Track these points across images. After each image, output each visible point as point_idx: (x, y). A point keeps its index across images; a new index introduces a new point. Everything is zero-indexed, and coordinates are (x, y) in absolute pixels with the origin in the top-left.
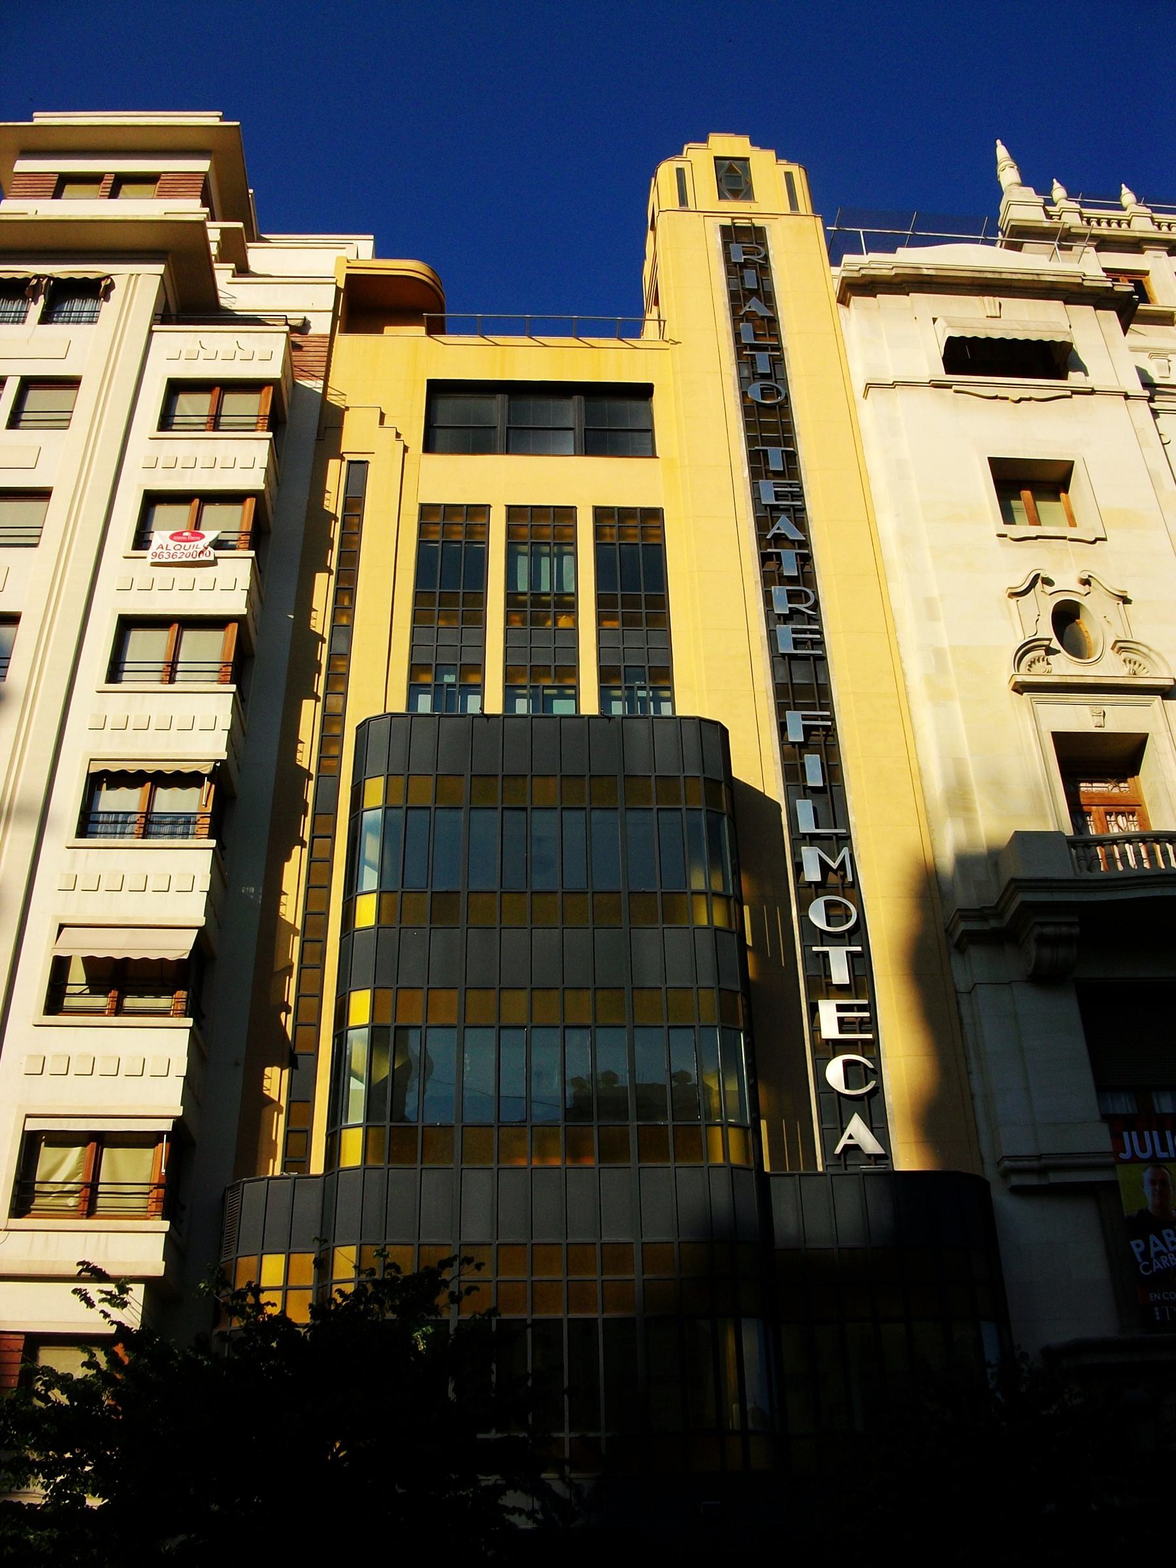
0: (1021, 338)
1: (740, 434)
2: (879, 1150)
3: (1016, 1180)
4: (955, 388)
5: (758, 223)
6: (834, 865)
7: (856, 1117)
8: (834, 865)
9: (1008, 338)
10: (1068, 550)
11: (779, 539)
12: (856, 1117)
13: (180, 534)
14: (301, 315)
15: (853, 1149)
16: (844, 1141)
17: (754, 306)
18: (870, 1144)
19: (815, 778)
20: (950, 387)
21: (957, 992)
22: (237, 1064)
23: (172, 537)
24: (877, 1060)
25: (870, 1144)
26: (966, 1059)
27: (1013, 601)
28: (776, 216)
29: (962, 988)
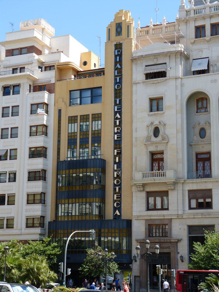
2: (119, 214)
5: (121, 42)
11: (117, 118)
15: (116, 214)
16: (115, 213)
18: (118, 214)
19: (117, 161)
24: (121, 203)
25: (118, 214)
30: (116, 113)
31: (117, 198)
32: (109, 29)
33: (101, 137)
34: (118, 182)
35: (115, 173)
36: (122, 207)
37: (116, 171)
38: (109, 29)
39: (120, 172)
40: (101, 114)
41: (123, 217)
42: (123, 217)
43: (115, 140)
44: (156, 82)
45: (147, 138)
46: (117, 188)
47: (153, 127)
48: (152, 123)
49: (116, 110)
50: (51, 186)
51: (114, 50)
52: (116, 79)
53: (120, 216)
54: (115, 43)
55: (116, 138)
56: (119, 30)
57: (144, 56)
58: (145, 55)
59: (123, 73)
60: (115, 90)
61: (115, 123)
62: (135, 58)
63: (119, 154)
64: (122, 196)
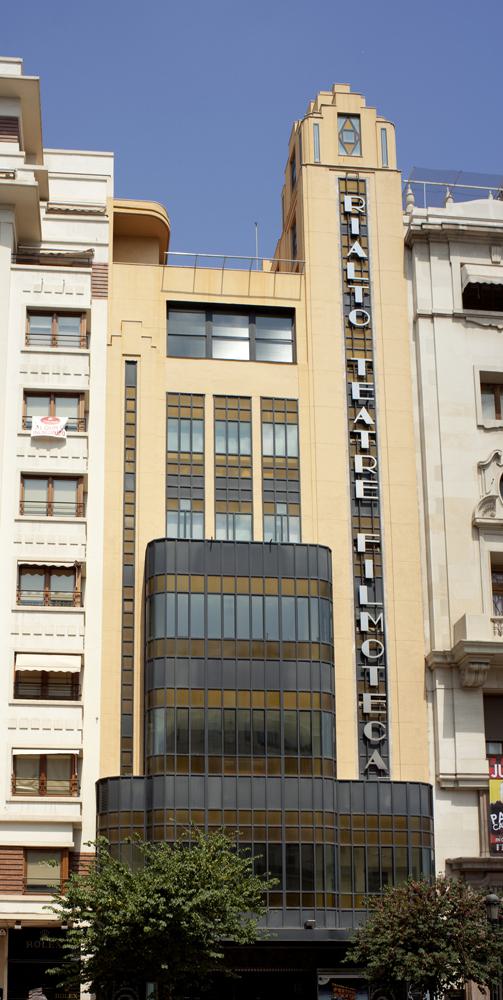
6: (376, 623)
8: (376, 623)
11: (362, 424)
13: (46, 419)
16: (370, 762)
17: (357, 248)
23: (42, 420)
30: (354, 405)
34: (375, 648)
54: (343, 175)
55: (360, 494)
59: (374, 277)
63: (374, 547)
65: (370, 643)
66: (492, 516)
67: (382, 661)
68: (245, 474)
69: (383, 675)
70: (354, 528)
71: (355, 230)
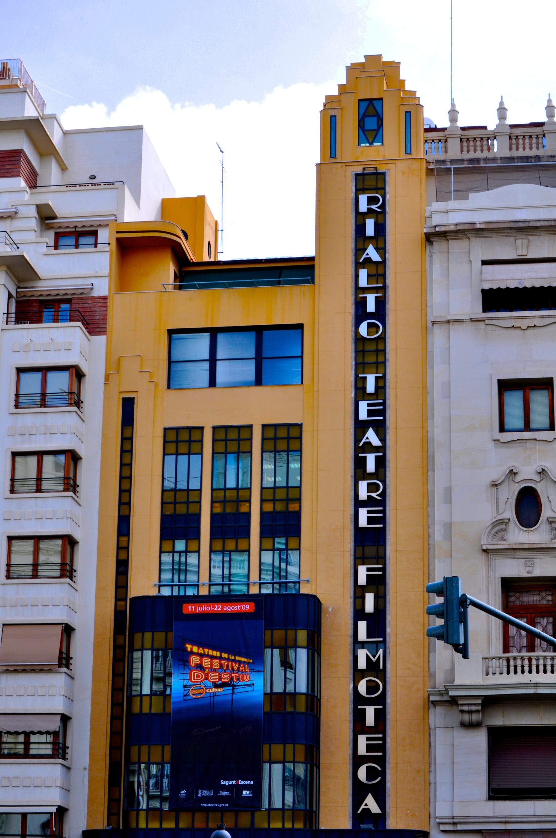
0: (529, 286)
1: (352, 362)
3: (443, 827)
4: (487, 322)
5: (381, 169)
6: (374, 660)
7: (370, 795)
8: (374, 660)
9: (521, 286)
10: (536, 448)
12: (370, 795)
14: (89, 281)
15: (367, 811)
16: (363, 807)
17: (372, 253)
19: (369, 607)
20: (484, 321)
21: (429, 728)
22: (85, 769)
26: (429, 764)
27: (494, 489)
28: (394, 162)
29: (432, 727)
31: (369, 748)
32: (333, 118)
33: (298, 515)
34: (372, 688)
35: (362, 654)
36: (388, 785)
37: (363, 645)
38: (333, 118)
39: (381, 652)
40: (299, 426)
41: (392, 824)
42: (392, 824)
43: (358, 531)
44: (524, 324)
45: (493, 527)
46: (370, 712)
47: (516, 489)
48: (512, 473)
49: (363, 415)
50: (503, 693)
51: (353, 195)
52: (360, 304)
53: (382, 817)
54: (359, 170)
55: (363, 522)
56: (371, 123)
57: (478, 226)
58: (485, 223)
59: (390, 281)
60: (358, 339)
61: (360, 463)
62: (443, 229)
64: (388, 740)
65: (368, 681)
66: (503, 539)
67: (382, 700)
68: (244, 509)
69: (381, 716)
70: (355, 558)
71: (370, 231)
